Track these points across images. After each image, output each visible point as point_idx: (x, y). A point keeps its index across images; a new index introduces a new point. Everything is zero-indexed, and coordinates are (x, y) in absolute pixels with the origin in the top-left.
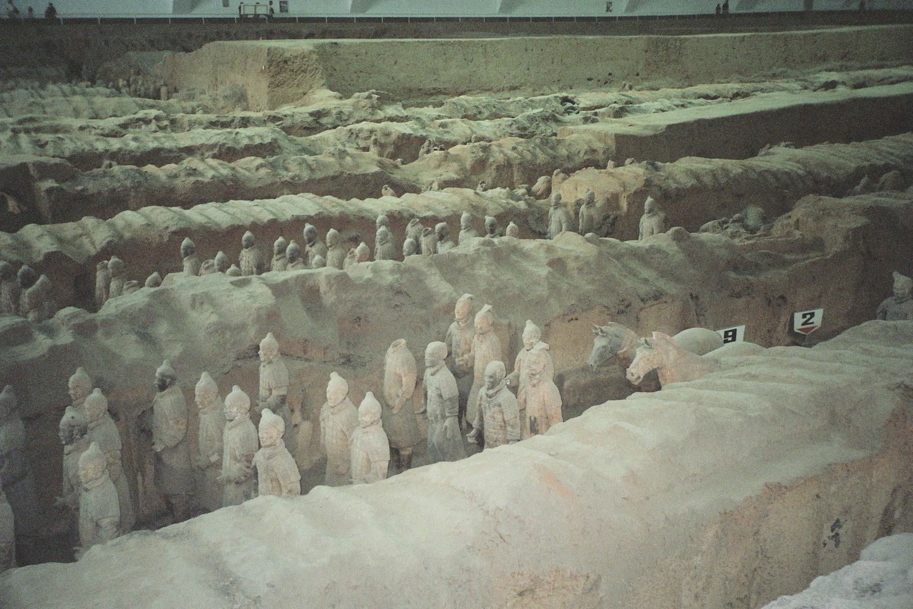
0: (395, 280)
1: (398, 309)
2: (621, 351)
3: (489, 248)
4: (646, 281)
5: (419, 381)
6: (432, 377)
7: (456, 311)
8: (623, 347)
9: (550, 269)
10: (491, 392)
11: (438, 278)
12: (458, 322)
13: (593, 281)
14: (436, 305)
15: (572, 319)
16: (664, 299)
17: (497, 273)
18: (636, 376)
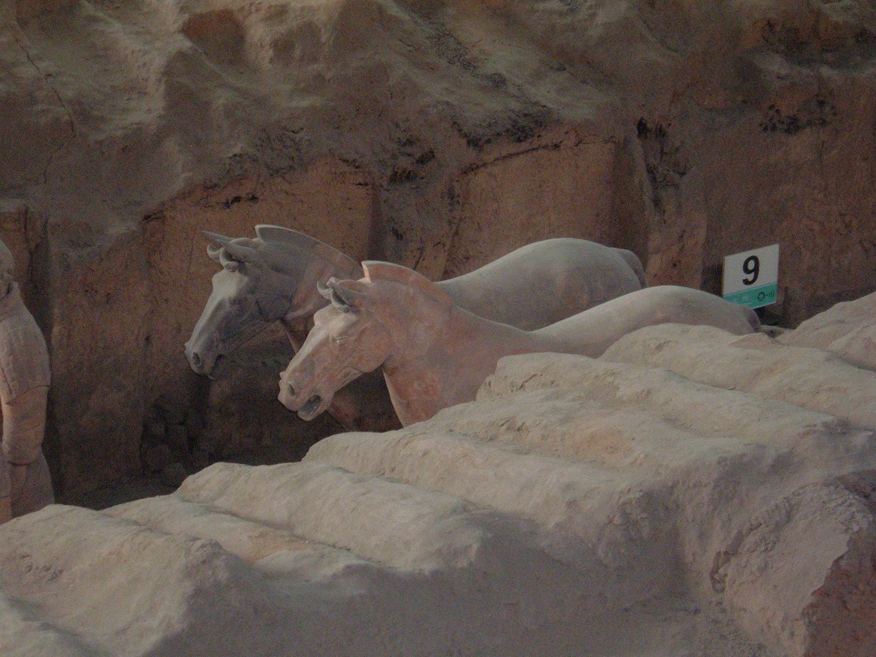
4: (498, 82)
8: (304, 301)
9: (185, 44)
15: (237, 199)
16: (548, 138)
18: (304, 396)
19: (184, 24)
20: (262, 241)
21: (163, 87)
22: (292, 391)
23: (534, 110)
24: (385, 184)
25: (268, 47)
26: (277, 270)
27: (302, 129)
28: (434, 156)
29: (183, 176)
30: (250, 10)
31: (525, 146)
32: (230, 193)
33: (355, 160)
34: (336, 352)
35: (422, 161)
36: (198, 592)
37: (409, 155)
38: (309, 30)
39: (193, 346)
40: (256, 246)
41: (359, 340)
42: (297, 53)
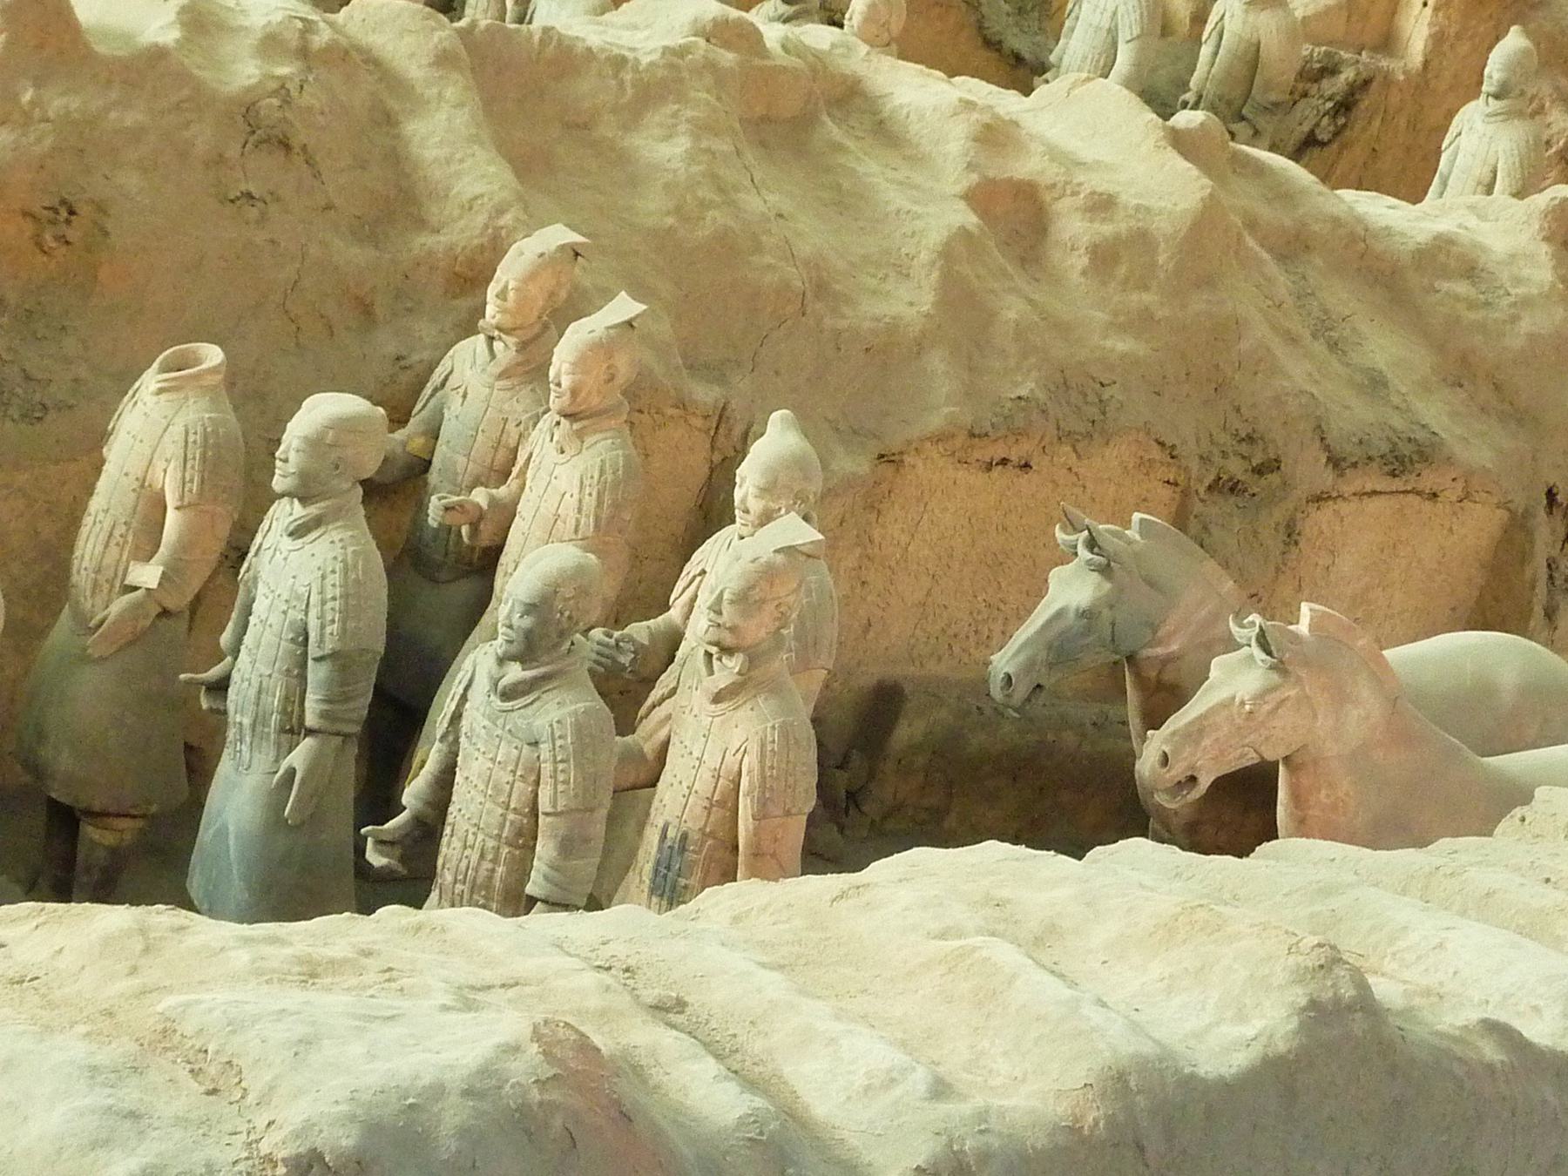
0: (273, 85)
1: (253, 213)
2: (1160, 651)
3: (728, 58)
4: (1375, 384)
5: (236, 553)
6: (287, 543)
7: (492, 290)
8: (1170, 635)
9: (971, 220)
10: (515, 673)
11: (462, 118)
12: (491, 339)
13: (1142, 322)
14: (423, 241)
15: (1004, 462)
16: (1428, 481)
17: (729, 174)
18: (1178, 771)
19: (1476, 245)
20: (1138, 537)
21: (935, 275)
22: (1165, 760)
23: (1420, 435)
24: (1202, 490)
25: (1082, 251)
26: (1151, 584)
28: (1278, 468)
29: (946, 410)
31: (1397, 484)
32: (999, 451)
33: (1173, 447)
34: (1238, 721)
35: (1259, 471)
36: (1314, 1004)
38: (1142, 240)
39: (1003, 661)
40: (1130, 542)
42: (1122, 270)
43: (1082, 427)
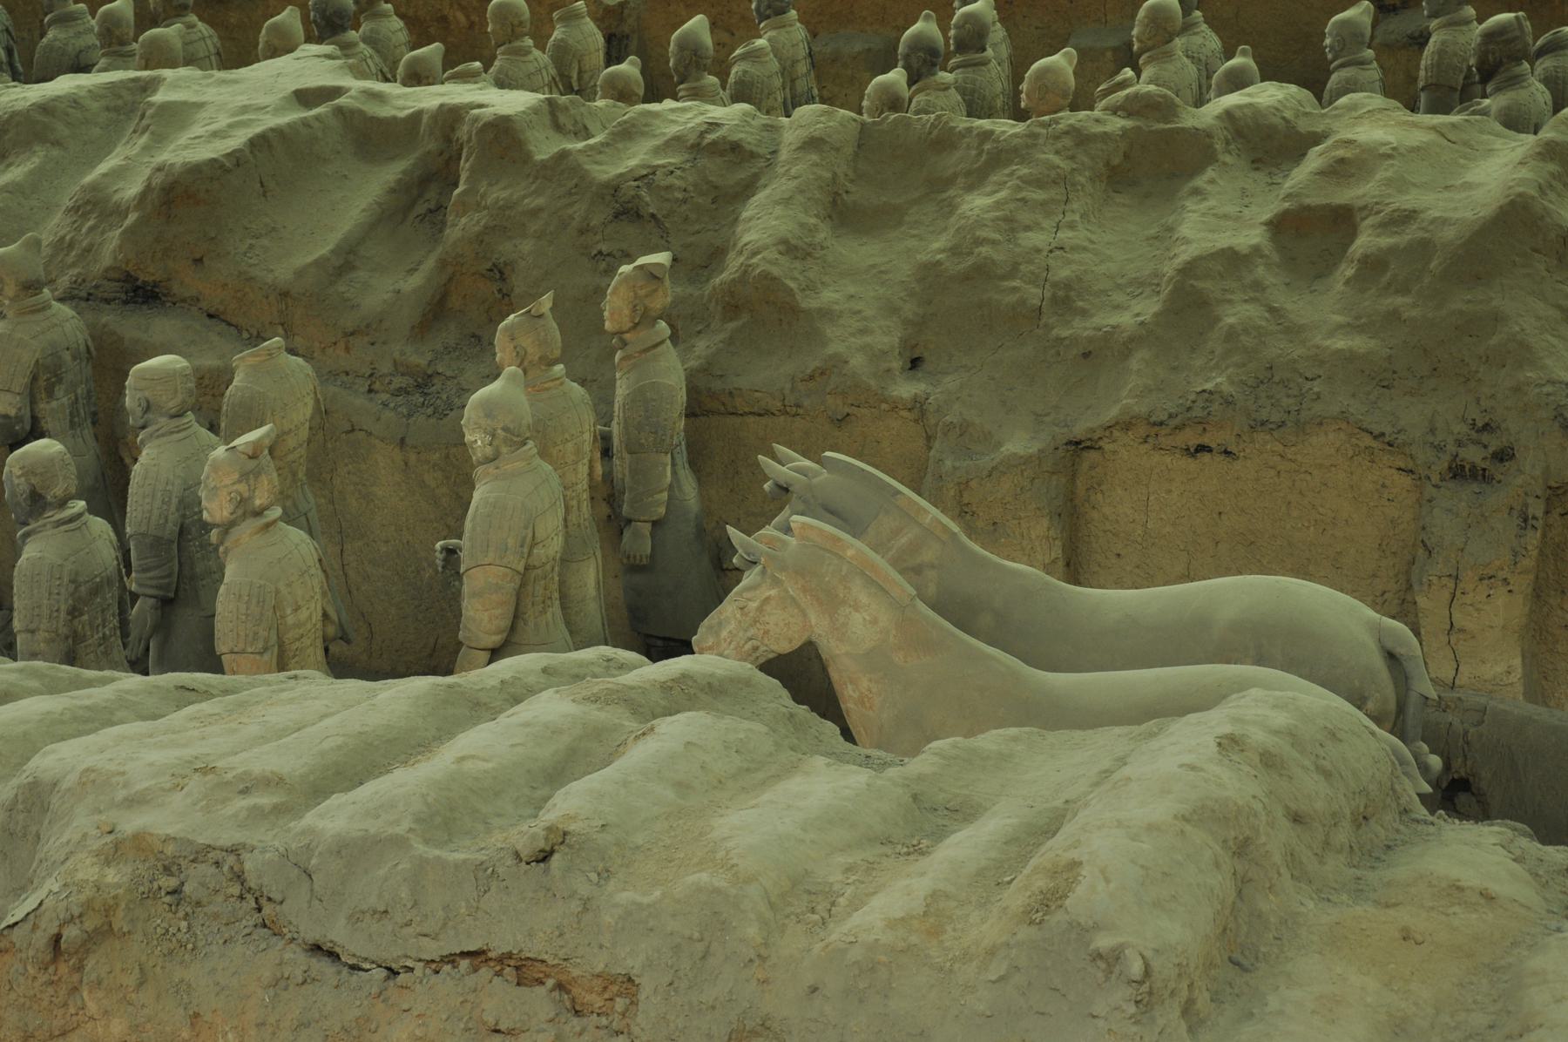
15: (1202, 448)
27: (1320, 377)
29: (1124, 402)
30: (1372, 208)
32: (1191, 438)
37: (1485, 447)
41: (760, 609)
43: (1276, 417)
